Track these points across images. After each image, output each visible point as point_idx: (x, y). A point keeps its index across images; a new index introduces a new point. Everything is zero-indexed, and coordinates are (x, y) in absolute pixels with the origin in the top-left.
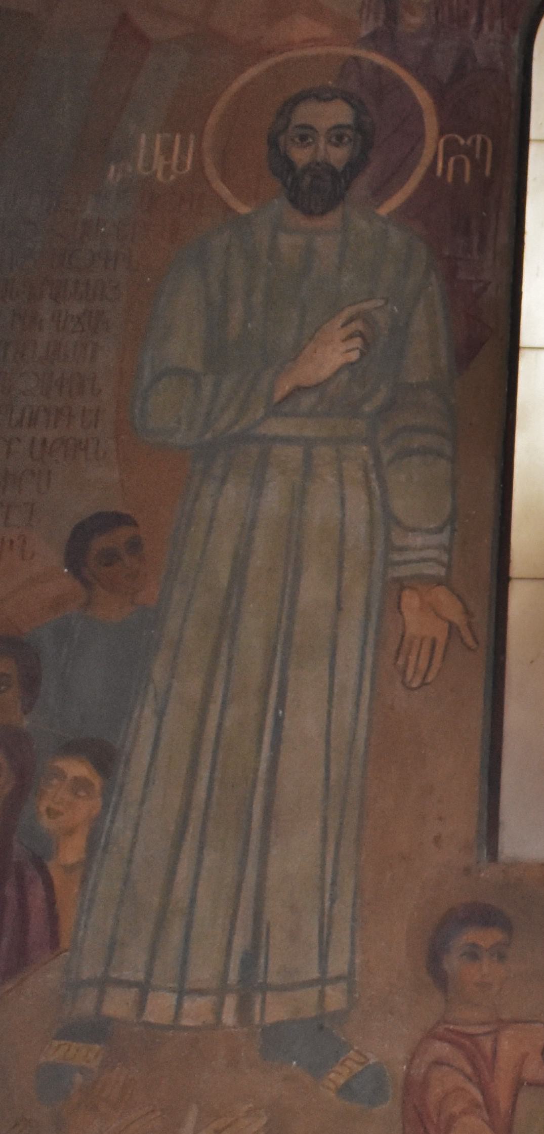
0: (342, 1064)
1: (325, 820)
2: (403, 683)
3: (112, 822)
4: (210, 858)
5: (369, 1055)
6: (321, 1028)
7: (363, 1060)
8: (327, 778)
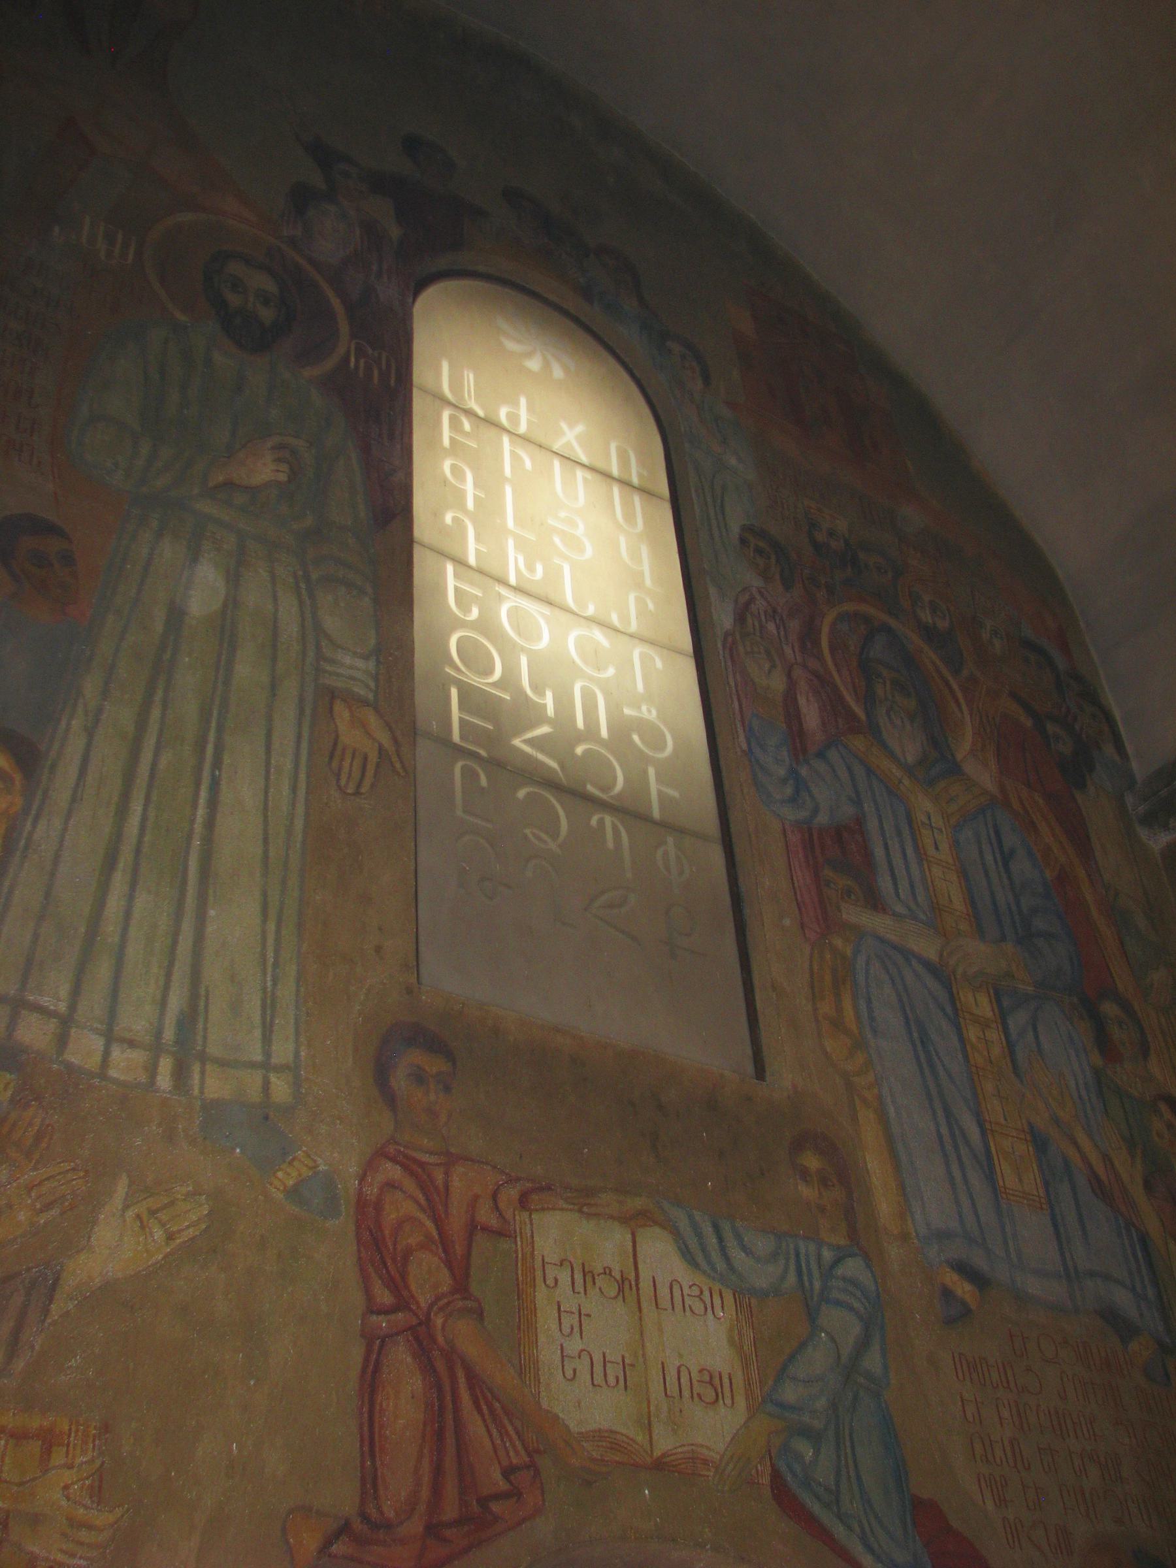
0: (291, 1163)
1: (265, 894)
2: (339, 787)
3: (34, 826)
4: (142, 901)
5: (320, 1161)
6: (266, 1118)
7: (311, 1164)
8: (266, 852)
